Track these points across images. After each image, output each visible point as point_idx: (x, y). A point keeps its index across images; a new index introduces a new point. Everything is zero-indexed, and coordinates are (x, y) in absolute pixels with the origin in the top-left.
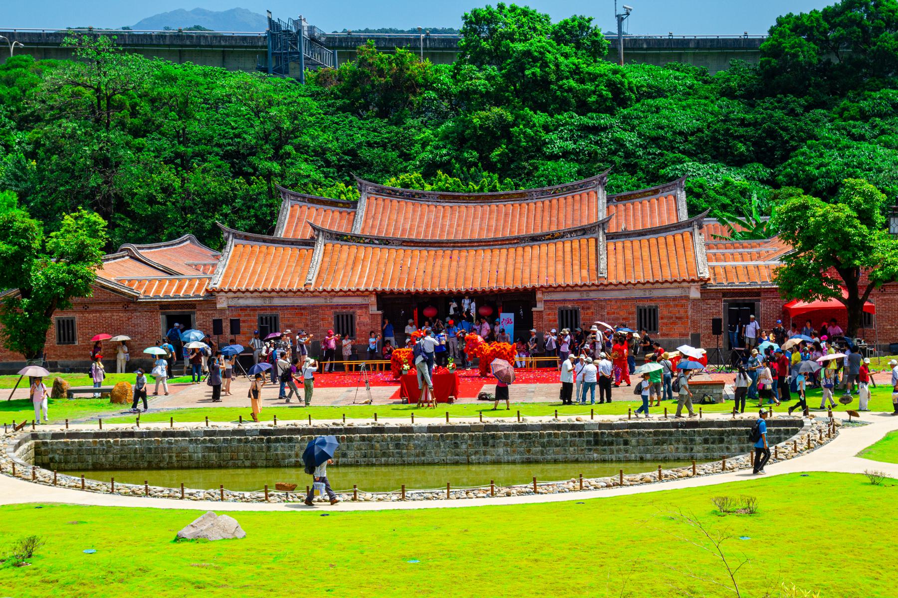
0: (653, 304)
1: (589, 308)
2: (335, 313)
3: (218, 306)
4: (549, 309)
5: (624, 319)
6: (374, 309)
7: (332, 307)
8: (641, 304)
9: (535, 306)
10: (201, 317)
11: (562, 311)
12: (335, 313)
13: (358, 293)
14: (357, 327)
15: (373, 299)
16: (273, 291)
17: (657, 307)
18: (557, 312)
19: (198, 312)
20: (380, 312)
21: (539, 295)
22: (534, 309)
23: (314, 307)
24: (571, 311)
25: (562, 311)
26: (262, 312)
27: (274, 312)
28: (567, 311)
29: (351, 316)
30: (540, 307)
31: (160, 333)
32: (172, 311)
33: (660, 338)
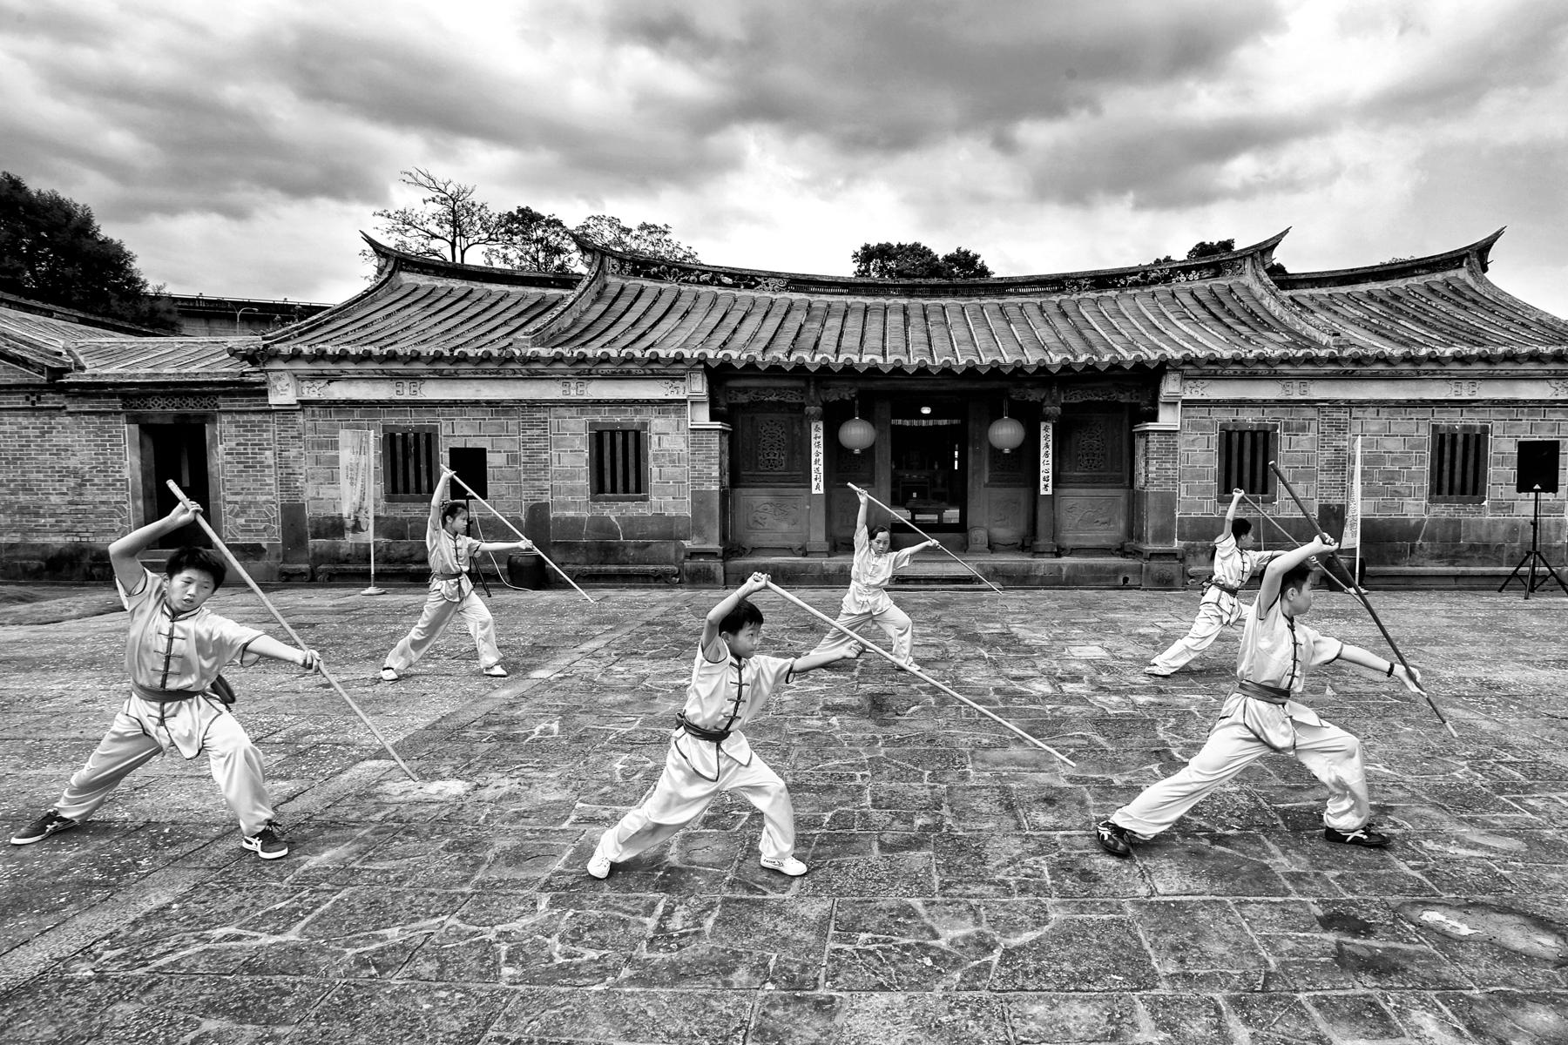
0: (1474, 419)
1: (1303, 429)
2: (592, 425)
3: (274, 399)
4: (1194, 426)
5: (1395, 460)
6: (701, 417)
7: (582, 404)
8: (1446, 419)
9: (1154, 417)
10: (233, 430)
11: (1229, 434)
12: (592, 425)
13: (656, 369)
14: (653, 469)
15: (698, 386)
16: (416, 357)
17: (1485, 430)
18: (1215, 437)
19: (225, 418)
20: (717, 425)
21: (1170, 387)
22: (1151, 426)
23: (533, 404)
24: (1254, 434)
25: (1229, 434)
26: (393, 420)
27: (425, 419)
28: (1242, 433)
29: (637, 433)
30: (1168, 418)
31: (126, 473)
32: (159, 410)
33: (1488, 517)
